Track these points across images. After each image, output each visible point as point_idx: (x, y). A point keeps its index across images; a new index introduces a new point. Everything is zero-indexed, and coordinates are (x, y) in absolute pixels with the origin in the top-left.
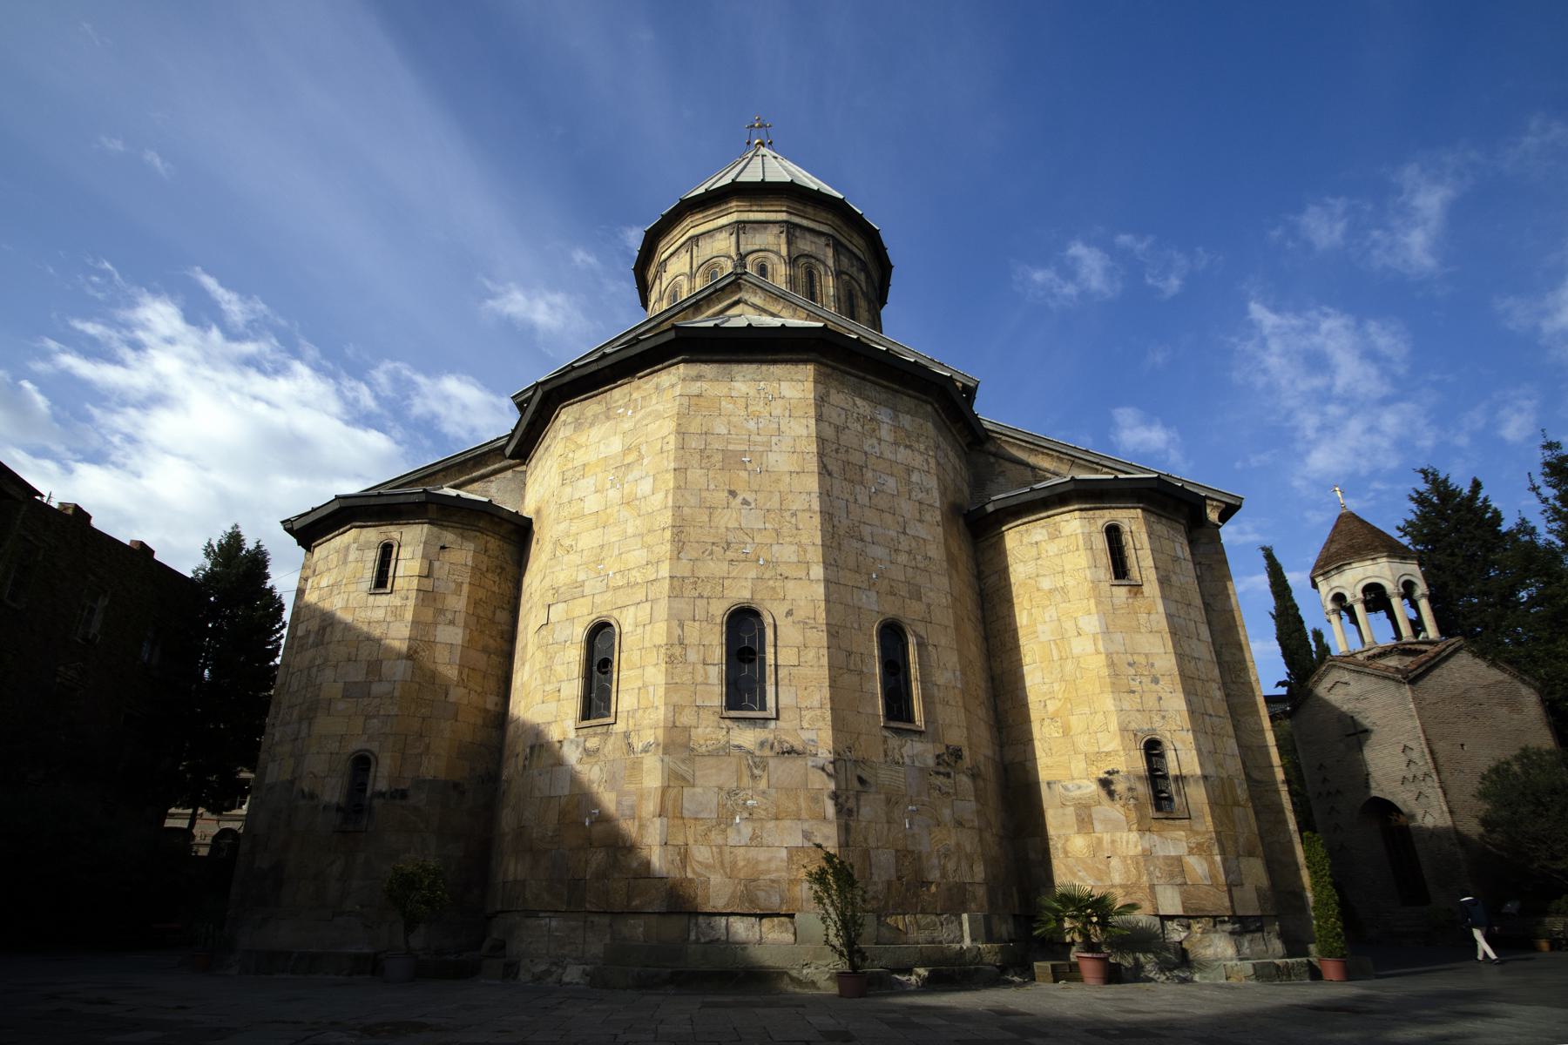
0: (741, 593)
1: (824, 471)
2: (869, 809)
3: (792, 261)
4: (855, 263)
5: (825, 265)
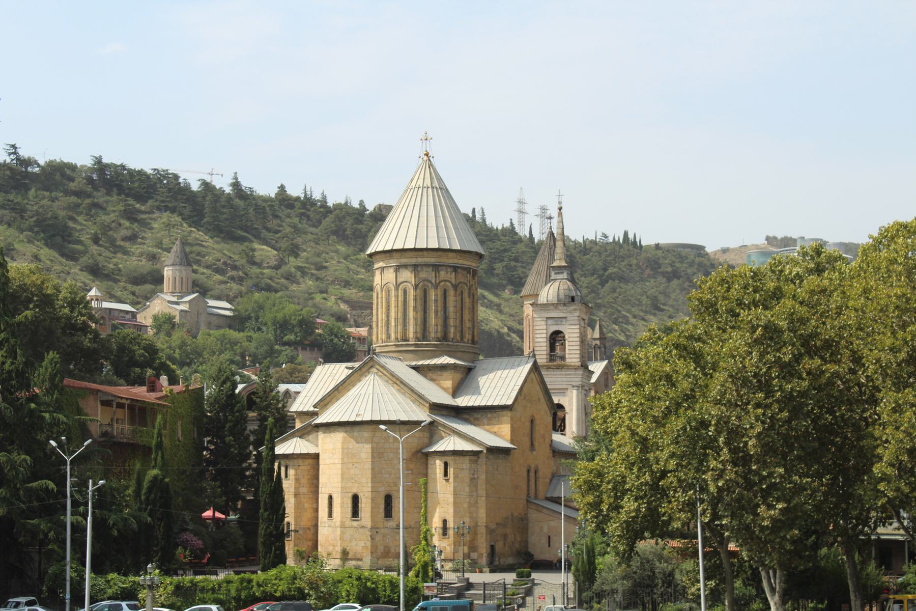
0: (354, 491)
1: (373, 457)
2: (378, 538)
3: (416, 287)
4: (449, 270)
5: (432, 283)
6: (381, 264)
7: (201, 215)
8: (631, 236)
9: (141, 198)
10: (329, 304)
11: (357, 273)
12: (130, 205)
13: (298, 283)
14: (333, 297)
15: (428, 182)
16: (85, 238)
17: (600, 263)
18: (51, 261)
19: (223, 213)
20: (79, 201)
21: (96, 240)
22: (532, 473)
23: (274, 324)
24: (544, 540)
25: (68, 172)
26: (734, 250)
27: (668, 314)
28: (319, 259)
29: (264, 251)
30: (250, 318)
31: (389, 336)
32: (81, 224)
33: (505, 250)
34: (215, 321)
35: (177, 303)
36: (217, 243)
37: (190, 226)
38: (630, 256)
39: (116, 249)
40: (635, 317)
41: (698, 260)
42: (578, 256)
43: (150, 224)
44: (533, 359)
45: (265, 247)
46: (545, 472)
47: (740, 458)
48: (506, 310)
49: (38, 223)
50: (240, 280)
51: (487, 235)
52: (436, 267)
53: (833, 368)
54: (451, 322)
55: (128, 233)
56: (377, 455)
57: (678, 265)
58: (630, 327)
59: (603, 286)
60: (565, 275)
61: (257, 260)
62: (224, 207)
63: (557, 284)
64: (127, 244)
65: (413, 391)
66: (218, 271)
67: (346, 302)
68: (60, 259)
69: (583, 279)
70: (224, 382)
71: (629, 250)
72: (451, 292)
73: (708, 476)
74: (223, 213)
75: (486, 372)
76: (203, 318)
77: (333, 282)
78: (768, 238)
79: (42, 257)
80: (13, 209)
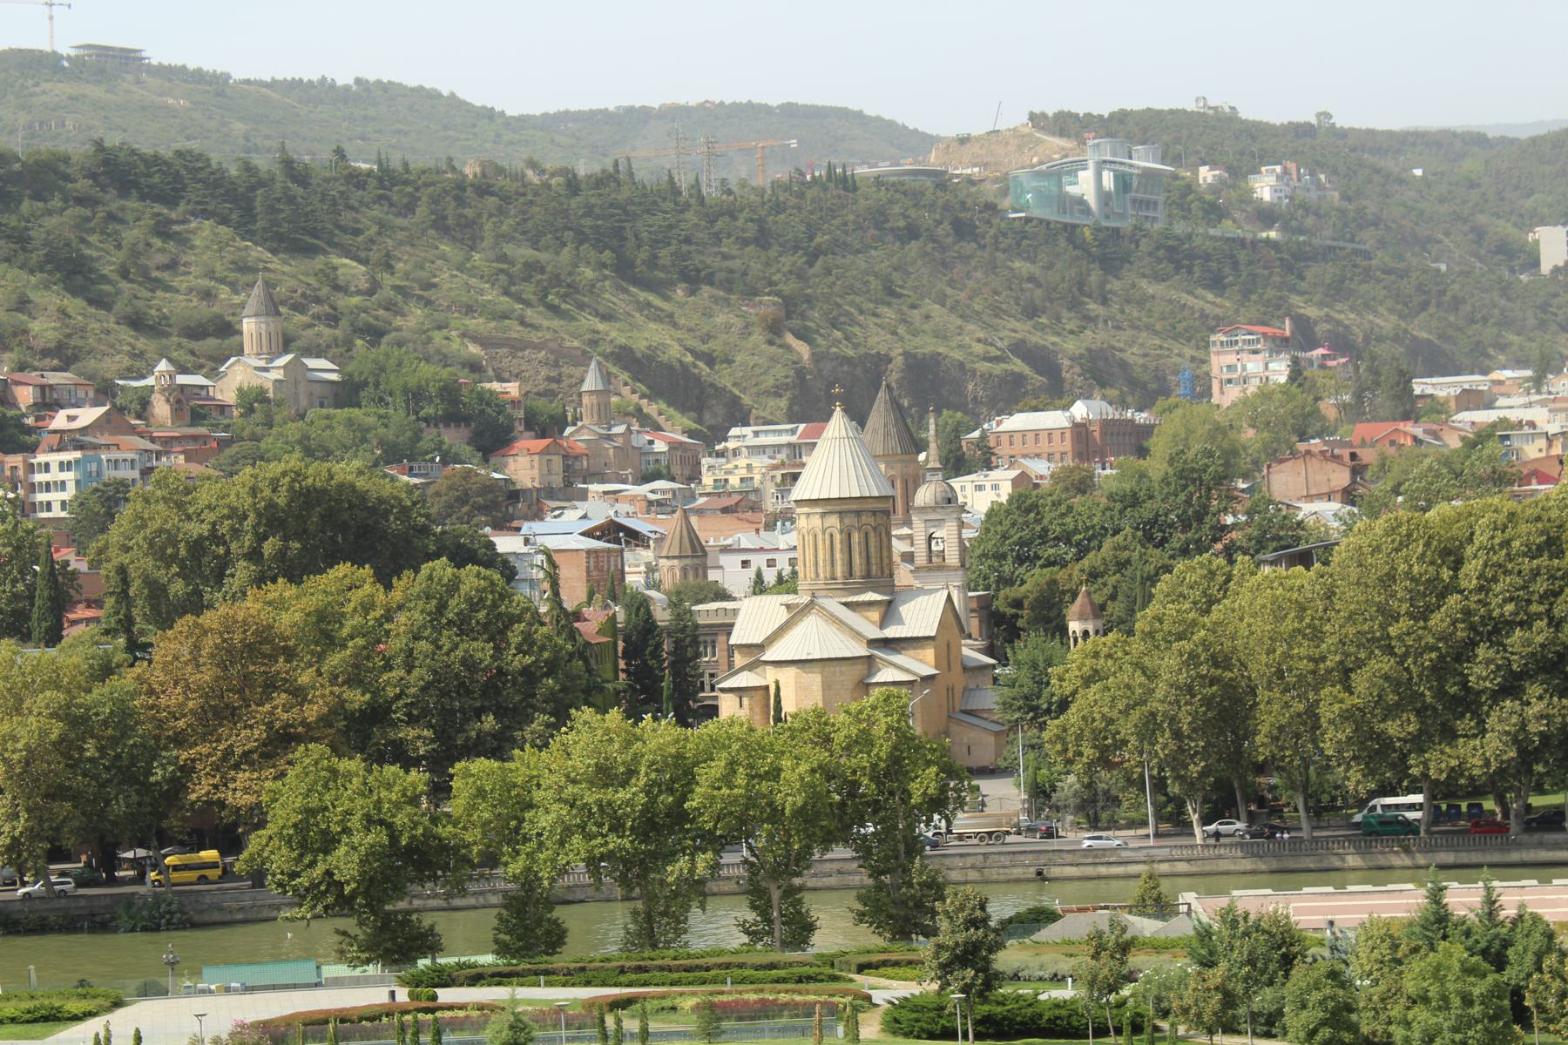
3: (841, 532)
6: (806, 510)
7: (248, 214)
8: (839, 170)
9: (171, 200)
10: (455, 345)
11: (481, 292)
12: (158, 215)
13: (403, 315)
14: (454, 333)
15: (843, 433)
16: (106, 270)
17: (802, 228)
18: (85, 316)
19: (280, 211)
20: (87, 212)
21: (124, 274)
22: (950, 690)
23: (405, 390)
24: (965, 750)
25: (62, 167)
26: (979, 138)
27: (909, 301)
28: (424, 274)
29: (350, 269)
30: (365, 384)
31: (817, 575)
32: (98, 249)
33: (670, 227)
34: (318, 390)
35: (266, 370)
36: (285, 262)
37: (243, 239)
38: (843, 207)
39: (157, 284)
40: (861, 312)
41: (943, 198)
42: (770, 219)
43: (189, 240)
44: (945, 593)
45: (347, 261)
46: (959, 689)
47: (1177, 735)
48: (682, 321)
49: (49, 258)
50: (333, 319)
51: (640, 204)
52: (858, 513)
53: (1228, 675)
54: (873, 561)
55: (161, 259)
56: (826, 687)
57: (912, 213)
58: (857, 330)
59: (811, 264)
60: (940, 477)
61: (340, 283)
62: (279, 200)
63: (933, 486)
64: (166, 276)
65: (851, 629)
66: (298, 308)
67: (475, 339)
68: (93, 310)
69: (782, 259)
70: (638, 609)
71: (839, 197)
72: (872, 534)
73: (1158, 747)
74: (280, 211)
75: (905, 602)
76: (302, 388)
77: (449, 308)
78: (1033, 117)
79: (70, 310)
80: (8, 237)
